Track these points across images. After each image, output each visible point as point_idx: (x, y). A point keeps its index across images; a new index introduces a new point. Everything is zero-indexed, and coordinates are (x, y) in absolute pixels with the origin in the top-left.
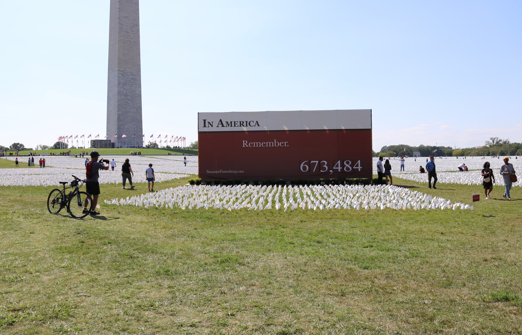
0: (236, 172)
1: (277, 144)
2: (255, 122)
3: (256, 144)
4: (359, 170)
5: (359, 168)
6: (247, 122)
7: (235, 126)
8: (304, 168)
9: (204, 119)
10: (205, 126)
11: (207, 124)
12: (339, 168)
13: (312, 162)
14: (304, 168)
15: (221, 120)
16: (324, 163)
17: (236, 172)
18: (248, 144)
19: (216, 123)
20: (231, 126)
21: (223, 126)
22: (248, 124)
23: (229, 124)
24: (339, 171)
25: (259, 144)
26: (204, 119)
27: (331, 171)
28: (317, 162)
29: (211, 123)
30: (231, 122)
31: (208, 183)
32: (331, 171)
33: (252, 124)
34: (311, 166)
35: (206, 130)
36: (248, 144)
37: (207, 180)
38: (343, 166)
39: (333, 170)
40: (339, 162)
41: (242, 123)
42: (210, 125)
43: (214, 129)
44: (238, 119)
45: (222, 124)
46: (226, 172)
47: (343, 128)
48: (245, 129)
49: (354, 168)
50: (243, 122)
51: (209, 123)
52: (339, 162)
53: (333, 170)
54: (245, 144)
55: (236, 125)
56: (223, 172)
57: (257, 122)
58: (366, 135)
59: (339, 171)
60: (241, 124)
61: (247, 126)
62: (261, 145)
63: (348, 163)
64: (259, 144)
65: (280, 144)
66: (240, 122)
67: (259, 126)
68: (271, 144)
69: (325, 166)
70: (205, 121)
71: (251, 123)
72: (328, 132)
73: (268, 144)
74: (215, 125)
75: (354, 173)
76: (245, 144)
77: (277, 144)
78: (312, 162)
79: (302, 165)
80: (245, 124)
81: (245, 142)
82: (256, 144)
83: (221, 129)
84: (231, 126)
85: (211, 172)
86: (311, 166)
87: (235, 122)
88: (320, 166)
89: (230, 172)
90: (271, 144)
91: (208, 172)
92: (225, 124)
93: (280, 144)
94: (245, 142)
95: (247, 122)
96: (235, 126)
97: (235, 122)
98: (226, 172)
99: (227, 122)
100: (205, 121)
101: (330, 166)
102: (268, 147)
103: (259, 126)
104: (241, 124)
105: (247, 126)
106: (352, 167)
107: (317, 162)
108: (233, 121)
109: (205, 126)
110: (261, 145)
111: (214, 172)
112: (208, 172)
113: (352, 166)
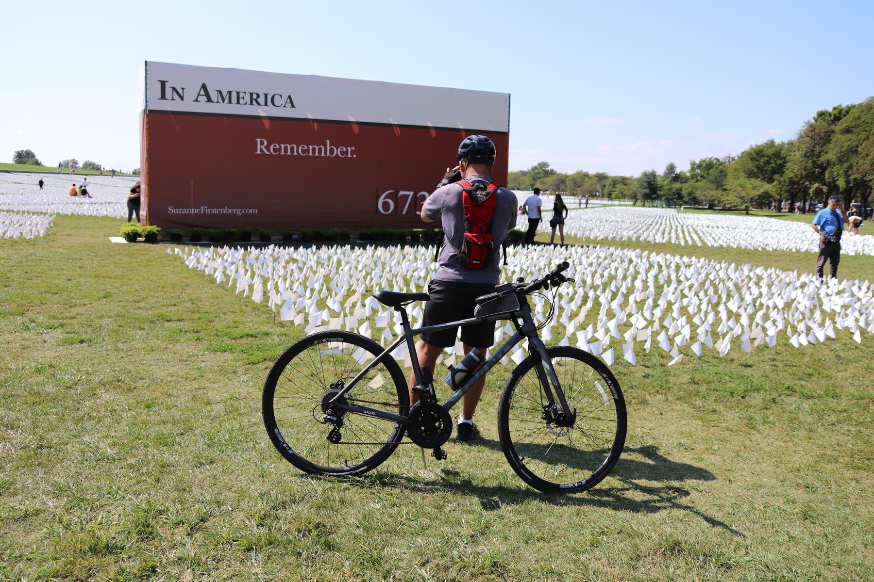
0: (239, 212)
1: (332, 151)
2: (285, 97)
3: (286, 149)
6: (266, 95)
7: (238, 102)
8: (386, 206)
9: (160, 79)
10: (163, 97)
11: (169, 92)
13: (402, 193)
14: (386, 206)
15: (204, 87)
19: (191, 93)
20: (230, 102)
21: (209, 100)
23: (225, 97)
25: (292, 148)
26: (160, 79)
28: (411, 193)
29: (180, 91)
30: (230, 93)
31: (176, 239)
33: (277, 100)
34: (399, 202)
37: (175, 231)
41: (255, 96)
42: (176, 96)
43: (188, 106)
44: (247, 88)
45: (207, 94)
46: (215, 211)
47: (461, 127)
48: (261, 111)
50: (258, 96)
51: (174, 89)
54: (261, 146)
55: (241, 101)
56: (208, 211)
57: (289, 97)
60: (254, 99)
61: (266, 104)
64: (292, 148)
65: (337, 152)
66: (251, 94)
67: (293, 106)
68: (320, 150)
70: (163, 84)
71: (277, 98)
72: (433, 133)
73: (314, 149)
76: (261, 146)
77: (332, 151)
78: (402, 193)
80: (261, 100)
81: (262, 143)
82: (286, 149)
83: (203, 107)
84: (230, 102)
86: (399, 202)
87: (238, 93)
89: (225, 211)
90: (320, 150)
91: (172, 210)
92: (214, 96)
93: (337, 152)
94: (262, 143)
95: (266, 95)
96: (238, 102)
97: (238, 93)
99: (220, 92)
100: (163, 84)
102: (314, 157)
103: (293, 106)
104: (254, 99)
105: (266, 104)
107: (411, 193)
108: (234, 90)
109: (163, 97)
112: (172, 210)
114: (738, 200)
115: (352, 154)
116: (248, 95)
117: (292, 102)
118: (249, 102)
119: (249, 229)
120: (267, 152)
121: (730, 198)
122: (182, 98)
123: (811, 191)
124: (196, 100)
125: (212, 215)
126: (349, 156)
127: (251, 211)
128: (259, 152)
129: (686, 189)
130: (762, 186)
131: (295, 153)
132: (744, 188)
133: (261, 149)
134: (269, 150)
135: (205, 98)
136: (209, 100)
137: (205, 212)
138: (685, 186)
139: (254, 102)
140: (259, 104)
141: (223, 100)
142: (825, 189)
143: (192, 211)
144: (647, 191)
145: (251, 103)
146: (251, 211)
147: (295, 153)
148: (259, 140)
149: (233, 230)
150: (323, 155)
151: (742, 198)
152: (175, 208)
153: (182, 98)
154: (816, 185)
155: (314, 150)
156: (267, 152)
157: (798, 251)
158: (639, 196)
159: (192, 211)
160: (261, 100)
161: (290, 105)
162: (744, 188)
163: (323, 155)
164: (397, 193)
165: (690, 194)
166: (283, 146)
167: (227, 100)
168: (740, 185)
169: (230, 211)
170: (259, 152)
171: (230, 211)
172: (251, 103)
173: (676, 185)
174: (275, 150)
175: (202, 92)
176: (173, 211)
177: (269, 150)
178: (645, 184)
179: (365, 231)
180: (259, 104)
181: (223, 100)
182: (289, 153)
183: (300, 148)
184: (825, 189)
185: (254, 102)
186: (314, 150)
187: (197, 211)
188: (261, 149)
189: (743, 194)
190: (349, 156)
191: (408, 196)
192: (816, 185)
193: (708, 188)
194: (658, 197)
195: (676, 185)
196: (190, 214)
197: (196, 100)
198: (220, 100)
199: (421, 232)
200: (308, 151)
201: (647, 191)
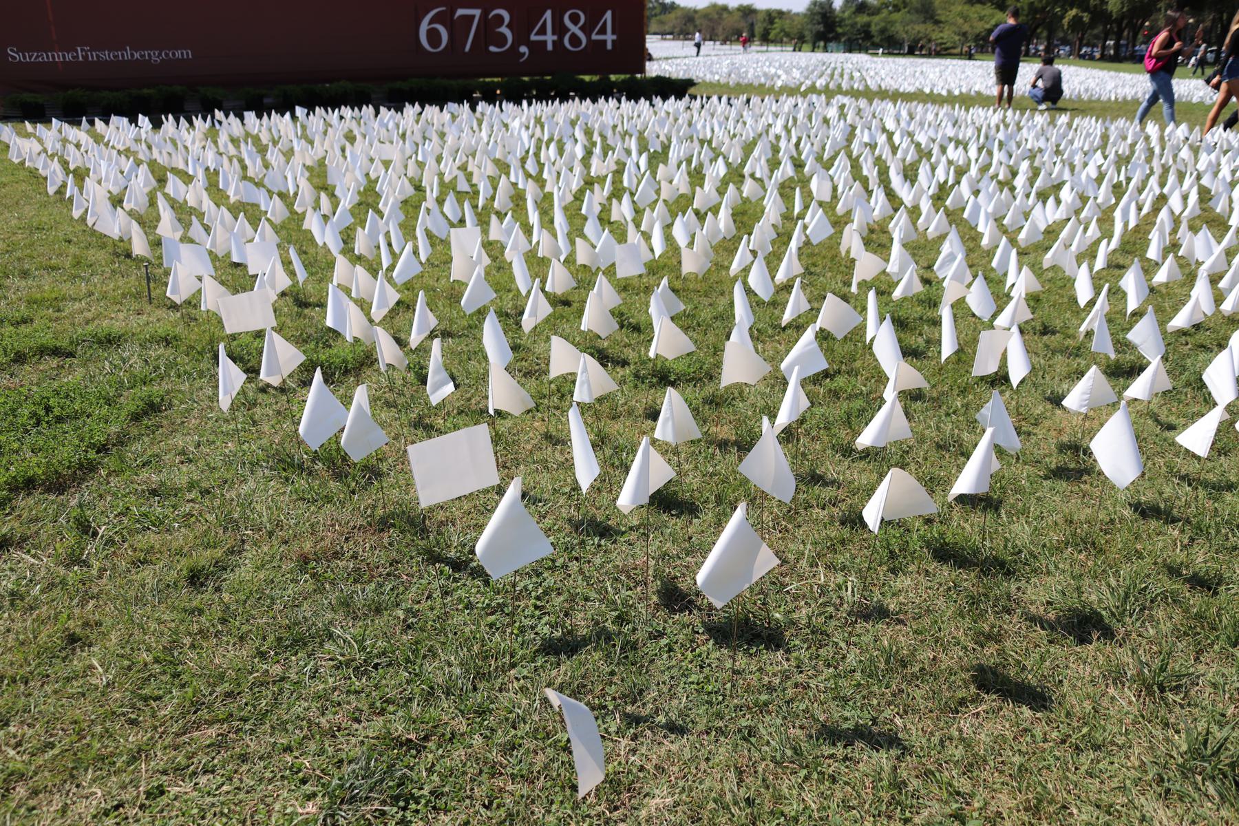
0: (155, 56)
4: (609, 46)
5: (609, 37)
8: (433, 36)
12: (550, 38)
16: (500, 19)
17: (155, 56)
24: (550, 47)
27: (523, 49)
28: (477, 13)
32: (523, 49)
34: (458, 28)
37: (27, 97)
38: (560, 29)
39: (531, 45)
40: (548, 14)
46: (107, 56)
49: (594, 37)
52: (548, 14)
53: (531, 45)
56: (93, 56)
59: (550, 47)
63: (575, 19)
69: (504, 30)
75: (596, 58)
79: (424, 27)
85: (32, 57)
86: (458, 28)
88: (488, 28)
89: (127, 54)
98: (107, 56)
101: (522, 28)
106: (588, 33)
111: (45, 57)
113: (587, 29)
114: (957, 38)
119: (178, 88)
121: (946, 35)
123: (1065, 21)
125: (100, 63)
127: (178, 54)
129: (876, 23)
130: (992, 16)
132: (966, 19)
137: (85, 57)
138: (876, 19)
142: (1086, 17)
143: (58, 57)
144: (821, 28)
146: (178, 54)
149: (146, 91)
151: (964, 34)
154: (1073, 12)
157: (1125, 99)
158: (808, 36)
159: (58, 57)
162: (966, 19)
164: (453, 12)
165: (883, 31)
168: (961, 15)
169: (137, 55)
171: (137, 55)
173: (862, 19)
176: (19, 57)
178: (818, 18)
179: (398, 84)
184: (1086, 17)
187: (69, 57)
189: (966, 28)
191: (473, 17)
192: (1073, 12)
193: (912, 21)
194: (837, 38)
195: (862, 19)
196: (54, 63)
199: (498, 85)
201: (821, 28)
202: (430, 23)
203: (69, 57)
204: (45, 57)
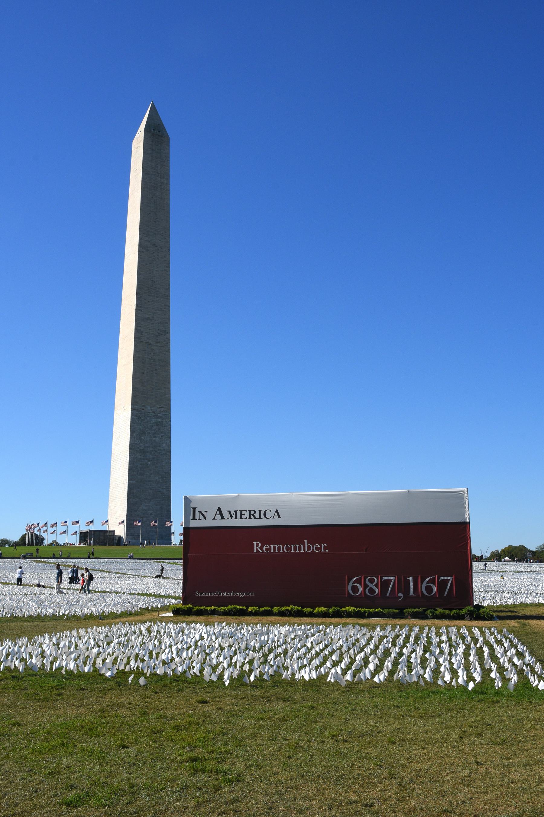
0: (241, 595)
1: (309, 548)
2: (274, 511)
3: (274, 548)
6: (260, 511)
7: (241, 518)
10: (194, 518)
11: (197, 514)
14: (355, 589)
15: (219, 509)
17: (241, 595)
18: (261, 548)
20: (236, 518)
21: (223, 518)
22: (263, 514)
23: (233, 515)
25: (279, 548)
30: (236, 512)
33: (268, 515)
35: (193, 524)
36: (261, 548)
41: (252, 513)
42: (202, 517)
44: (247, 507)
46: (226, 594)
50: (255, 512)
51: (201, 512)
54: (257, 547)
55: (243, 517)
56: (221, 594)
57: (277, 511)
58: (460, 531)
60: (252, 515)
61: (260, 518)
62: (284, 549)
64: (279, 548)
65: (313, 548)
66: (250, 511)
67: (279, 517)
68: (300, 547)
73: (295, 547)
74: (210, 516)
77: (309, 548)
80: (257, 515)
81: (257, 545)
84: (236, 518)
87: (241, 511)
89: (232, 594)
90: (300, 547)
92: (225, 515)
93: (313, 548)
94: (257, 545)
95: (260, 511)
96: (241, 518)
97: (241, 511)
98: (226, 594)
99: (229, 512)
100: (194, 509)
103: (279, 517)
105: (260, 518)
109: (194, 518)
110: (284, 549)
111: (206, 594)
115: (325, 549)
116: (248, 512)
117: (278, 515)
118: (248, 517)
120: (261, 551)
122: (205, 518)
124: (214, 519)
125: (224, 597)
126: (323, 551)
128: (255, 551)
131: (281, 551)
133: (257, 549)
134: (262, 550)
135: (220, 517)
136: (223, 518)
137: (218, 595)
139: (252, 517)
140: (255, 518)
141: (232, 517)
145: (250, 518)
146: (250, 594)
147: (281, 551)
148: (255, 543)
150: (302, 551)
152: (200, 592)
153: (205, 518)
155: (295, 548)
156: (261, 551)
160: (257, 515)
161: (277, 517)
163: (302, 551)
166: (272, 546)
167: (234, 517)
169: (235, 594)
170: (255, 551)
171: (235, 594)
172: (250, 518)
174: (266, 549)
175: (218, 513)
177: (262, 550)
180: (255, 518)
181: (232, 517)
182: (277, 551)
183: (285, 547)
185: (252, 517)
186: (295, 548)
187: (213, 594)
188: (257, 549)
190: (323, 551)
197: (214, 519)
198: (230, 517)
200: (270, 549)
202: (354, 583)
203: (213, 594)
204: (206, 594)
